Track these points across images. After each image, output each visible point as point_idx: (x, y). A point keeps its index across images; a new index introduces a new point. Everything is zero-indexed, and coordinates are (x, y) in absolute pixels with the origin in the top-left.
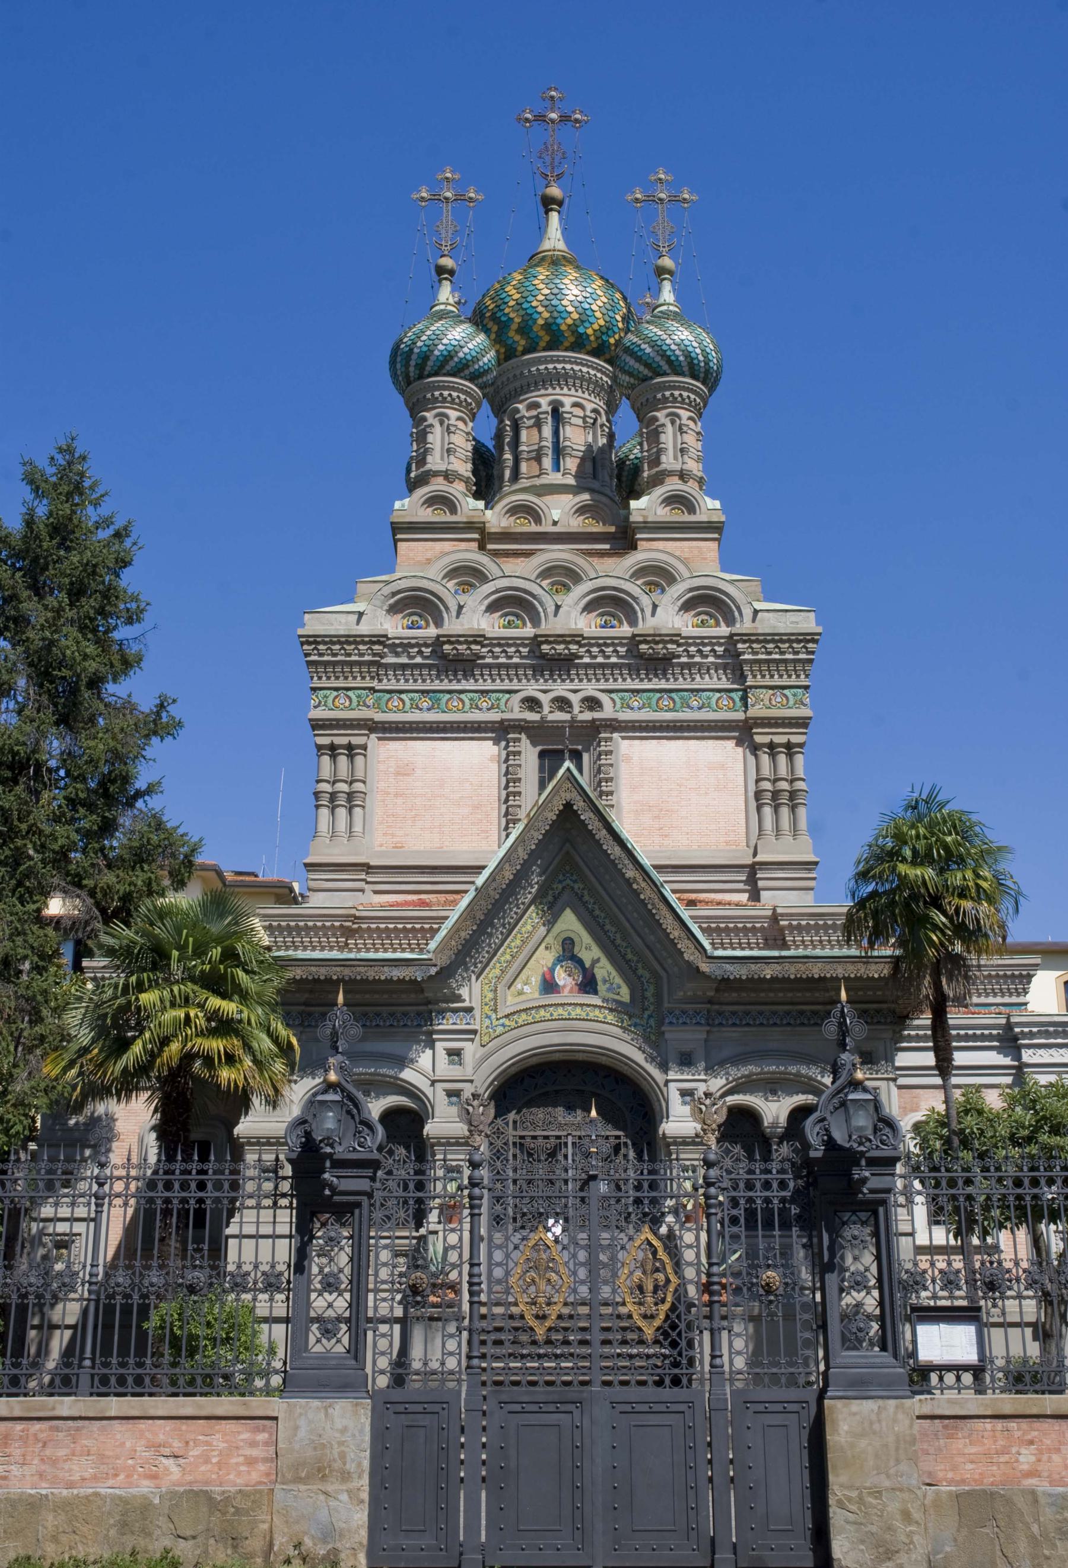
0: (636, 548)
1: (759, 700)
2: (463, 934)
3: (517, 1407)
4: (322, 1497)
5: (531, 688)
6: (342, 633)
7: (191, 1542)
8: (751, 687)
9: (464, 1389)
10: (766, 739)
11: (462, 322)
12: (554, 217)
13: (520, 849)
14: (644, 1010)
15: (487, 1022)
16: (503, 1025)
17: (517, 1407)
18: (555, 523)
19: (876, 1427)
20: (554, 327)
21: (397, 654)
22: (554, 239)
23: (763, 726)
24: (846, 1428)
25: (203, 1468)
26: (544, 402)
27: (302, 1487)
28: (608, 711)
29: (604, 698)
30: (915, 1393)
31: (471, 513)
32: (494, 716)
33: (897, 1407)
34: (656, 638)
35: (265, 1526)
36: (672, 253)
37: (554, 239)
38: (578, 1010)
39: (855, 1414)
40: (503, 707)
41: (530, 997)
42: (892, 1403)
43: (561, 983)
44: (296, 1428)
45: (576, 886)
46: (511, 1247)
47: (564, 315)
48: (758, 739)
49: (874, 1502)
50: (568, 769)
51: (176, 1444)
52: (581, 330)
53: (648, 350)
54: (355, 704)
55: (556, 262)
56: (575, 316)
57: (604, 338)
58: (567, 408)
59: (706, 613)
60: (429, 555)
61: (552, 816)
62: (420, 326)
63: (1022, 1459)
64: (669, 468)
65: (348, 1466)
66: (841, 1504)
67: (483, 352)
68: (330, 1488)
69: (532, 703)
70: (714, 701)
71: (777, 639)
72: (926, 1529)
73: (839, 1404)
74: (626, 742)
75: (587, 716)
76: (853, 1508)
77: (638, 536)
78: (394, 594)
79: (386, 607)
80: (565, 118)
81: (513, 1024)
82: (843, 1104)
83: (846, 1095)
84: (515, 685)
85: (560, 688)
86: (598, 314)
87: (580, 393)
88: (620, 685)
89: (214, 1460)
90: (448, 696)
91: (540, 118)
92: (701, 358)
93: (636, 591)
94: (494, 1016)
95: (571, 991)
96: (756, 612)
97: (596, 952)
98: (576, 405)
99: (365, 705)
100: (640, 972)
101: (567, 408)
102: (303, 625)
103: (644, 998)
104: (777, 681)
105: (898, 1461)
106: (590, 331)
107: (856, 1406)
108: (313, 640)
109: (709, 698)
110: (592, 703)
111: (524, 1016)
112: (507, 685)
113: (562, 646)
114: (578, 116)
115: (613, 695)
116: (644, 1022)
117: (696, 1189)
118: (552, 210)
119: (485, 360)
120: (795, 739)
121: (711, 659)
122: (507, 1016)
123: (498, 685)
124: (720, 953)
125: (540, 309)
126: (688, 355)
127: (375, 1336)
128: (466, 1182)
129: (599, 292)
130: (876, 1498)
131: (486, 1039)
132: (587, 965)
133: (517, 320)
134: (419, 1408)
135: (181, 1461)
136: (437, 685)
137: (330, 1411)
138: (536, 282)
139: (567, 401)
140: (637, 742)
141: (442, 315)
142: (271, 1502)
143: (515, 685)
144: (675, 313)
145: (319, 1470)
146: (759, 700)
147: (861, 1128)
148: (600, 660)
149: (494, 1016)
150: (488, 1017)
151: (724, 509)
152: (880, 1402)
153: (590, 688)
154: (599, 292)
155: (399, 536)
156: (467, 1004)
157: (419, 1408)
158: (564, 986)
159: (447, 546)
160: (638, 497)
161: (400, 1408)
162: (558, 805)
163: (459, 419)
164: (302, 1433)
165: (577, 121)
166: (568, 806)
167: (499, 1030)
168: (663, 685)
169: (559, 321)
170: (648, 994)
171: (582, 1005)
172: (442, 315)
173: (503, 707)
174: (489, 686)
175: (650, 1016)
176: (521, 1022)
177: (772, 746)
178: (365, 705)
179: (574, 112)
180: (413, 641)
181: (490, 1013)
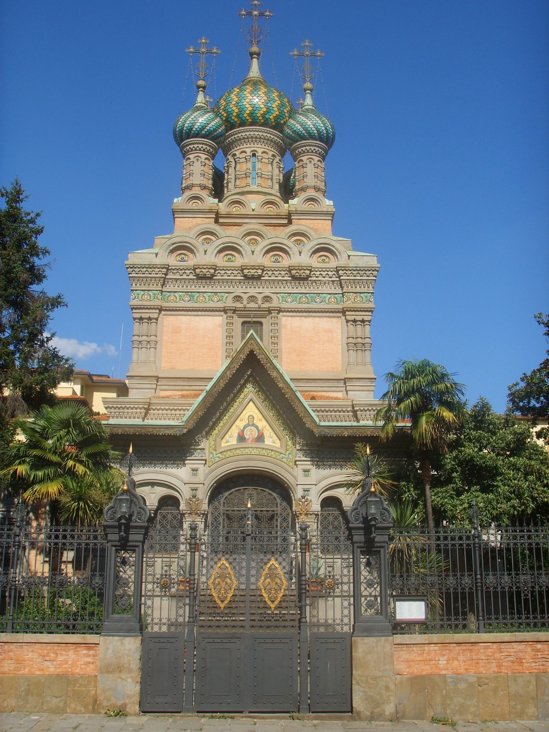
0: (291, 224)
2: (200, 413)
3: (211, 640)
4: (119, 680)
5: (239, 290)
6: (147, 263)
7: (59, 699)
8: (345, 292)
9: (186, 631)
10: (352, 318)
11: (209, 112)
12: (255, 61)
13: (228, 373)
14: (287, 450)
15: (211, 455)
17: (211, 640)
18: (253, 210)
19: (375, 649)
20: (254, 115)
22: (255, 71)
24: (362, 650)
25: (65, 666)
26: (248, 151)
27: (111, 676)
28: (275, 304)
29: (274, 296)
30: (394, 634)
31: (212, 205)
32: (221, 305)
33: (385, 640)
34: (300, 268)
35: (93, 692)
36: (311, 81)
37: (255, 71)
39: (366, 644)
40: (224, 300)
41: (232, 443)
42: (383, 638)
43: (247, 437)
44: (108, 649)
46: (209, 567)
47: (259, 109)
48: (349, 318)
49: (373, 682)
50: (252, 334)
51: (52, 655)
52: (267, 116)
53: (299, 127)
54: (152, 298)
55: (255, 84)
56: (265, 110)
57: (279, 120)
58: (259, 154)
60: (190, 225)
61: (243, 356)
62: (188, 114)
63: (440, 662)
64: (309, 184)
65: (131, 666)
66: (358, 683)
67: (219, 127)
68: (123, 676)
69: (238, 298)
70: (327, 299)
71: (358, 269)
72: (396, 694)
73: (359, 639)
74: (284, 318)
75: (266, 305)
76: (363, 685)
77: (293, 217)
78: (173, 244)
79: (168, 251)
80: (261, 14)
81: (224, 457)
82: (366, 502)
83: (367, 498)
84: (231, 290)
85: (252, 291)
86: (276, 109)
87: (266, 147)
88: (282, 290)
89: (70, 663)
90: (198, 294)
91: (249, 14)
92: (325, 132)
93: (291, 245)
94: (214, 453)
95: (252, 441)
96: (349, 256)
97: (264, 423)
98: (263, 152)
99: (157, 298)
101: (259, 154)
102: (127, 259)
103: (287, 445)
104: (358, 289)
105: (384, 665)
106: (271, 117)
107: (366, 640)
108: (133, 267)
109: (325, 298)
110: (267, 299)
111: (229, 453)
112: (227, 289)
113: (255, 271)
114: (267, 13)
115: (278, 295)
116: (286, 456)
117: (296, 541)
118: (254, 58)
119: (220, 130)
120: (366, 318)
121: (326, 279)
122: (221, 453)
123: (223, 289)
124: (322, 424)
125: (247, 106)
126: (318, 130)
127: (145, 607)
128: (189, 537)
129: (276, 98)
130: (374, 681)
131: (211, 464)
133: (237, 111)
134: (165, 640)
135: (55, 663)
136: (193, 289)
137: (124, 641)
138: (245, 93)
139: (260, 151)
140: (290, 318)
141: (199, 109)
142: (96, 682)
143: (231, 290)
144: (312, 109)
145: (118, 668)
147: (373, 514)
148: (273, 278)
149: (214, 453)
150: (212, 453)
151: (335, 206)
152: (378, 638)
153: (267, 291)
154: (276, 98)
155: (176, 216)
157: (165, 640)
158: (248, 439)
159: (199, 221)
160: (293, 198)
161: (157, 640)
162: (246, 351)
163: (206, 159)
164: (110, 652)
165: (266, 16)
166: (252, 352)
167: (217, 459)
168: (303, 290)
169: (257, 112)
171: (257, 448)
172: (199, 109)
173: (224, 300)
174: (218, 289)
175: (290, 454)
176: (227, 456)
177: (355, 321)
178: (157, 298)
179: (266, 11)
180: (181, 268)
181: (212, 451)
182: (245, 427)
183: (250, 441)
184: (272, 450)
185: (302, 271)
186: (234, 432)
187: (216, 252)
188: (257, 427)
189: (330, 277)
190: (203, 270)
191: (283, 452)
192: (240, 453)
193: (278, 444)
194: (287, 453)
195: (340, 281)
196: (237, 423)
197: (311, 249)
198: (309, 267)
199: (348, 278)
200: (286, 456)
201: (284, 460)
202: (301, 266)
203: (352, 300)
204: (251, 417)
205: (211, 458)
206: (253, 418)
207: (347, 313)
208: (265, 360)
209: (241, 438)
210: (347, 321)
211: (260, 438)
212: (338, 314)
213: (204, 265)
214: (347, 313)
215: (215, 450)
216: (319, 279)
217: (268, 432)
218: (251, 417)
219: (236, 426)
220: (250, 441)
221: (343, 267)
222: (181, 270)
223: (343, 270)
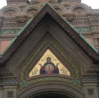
1: (94, 29)
2: (12, 50)
13: (32, 25)
14: (75, 77)
16: (27, 84)
21: (6, 21)
23: (95, 34)
38: (53, 78)
41: (37, 74)
43: (47, 71)
45: (51, 42)
59: (80, 11)
61: (42, 16)
70: (83, 29)
81: (31, 83)
94: (24, 81)
95: (50, 73)
97: (58, 61)
100: (73, 66)
103: (75, 74)
111: (34, 81)
116: (76, 81)
131: (21, 88)
132: (55, 65)
146: (94, 29)
149: (24, 81)
156: (15, 76)
162: (44, 14)
167: (26, 85)
170: (76, 73)
181: (23, 80)
182: (45, 64)
183: (49, 73)
184: (65, 78)
185: (69, 17)
186: (38, 67)
187: (27, 11)
188: (53, 64)
189: (84, 20)
190: (21, 19)
191: (73, 78)
192: (43, 80)
193: (68, 74)
194: (76, 79)
195: (89, 21)
196: (40, 62)
197: (73, 8)
198: (73, 15)
199: (92, 19)
200: (76, 81)
201: (74, 84)
202: (69, 15)
203: (96, 29)
204: (49, 59)
205: (22, 85)
206: (50, 58)
207: (94, 35)
208: (56, 18)
209: (43, 71)
210: (94, 39)
211: (56, 70)
212: (89, 36)
213: (21, 16)
214: (94, 35)
215: (24, 79)
216: (78, 20)
217: (61, 66)
218: (49, 59)
219: (39, 64)
220: (49, 73)
221: (90, 14)
222: (10, 19)
223: (89, 16)
